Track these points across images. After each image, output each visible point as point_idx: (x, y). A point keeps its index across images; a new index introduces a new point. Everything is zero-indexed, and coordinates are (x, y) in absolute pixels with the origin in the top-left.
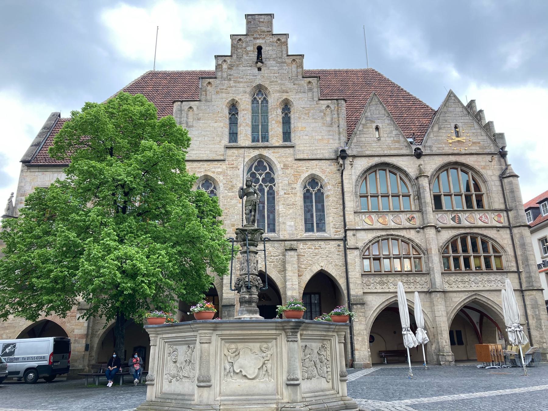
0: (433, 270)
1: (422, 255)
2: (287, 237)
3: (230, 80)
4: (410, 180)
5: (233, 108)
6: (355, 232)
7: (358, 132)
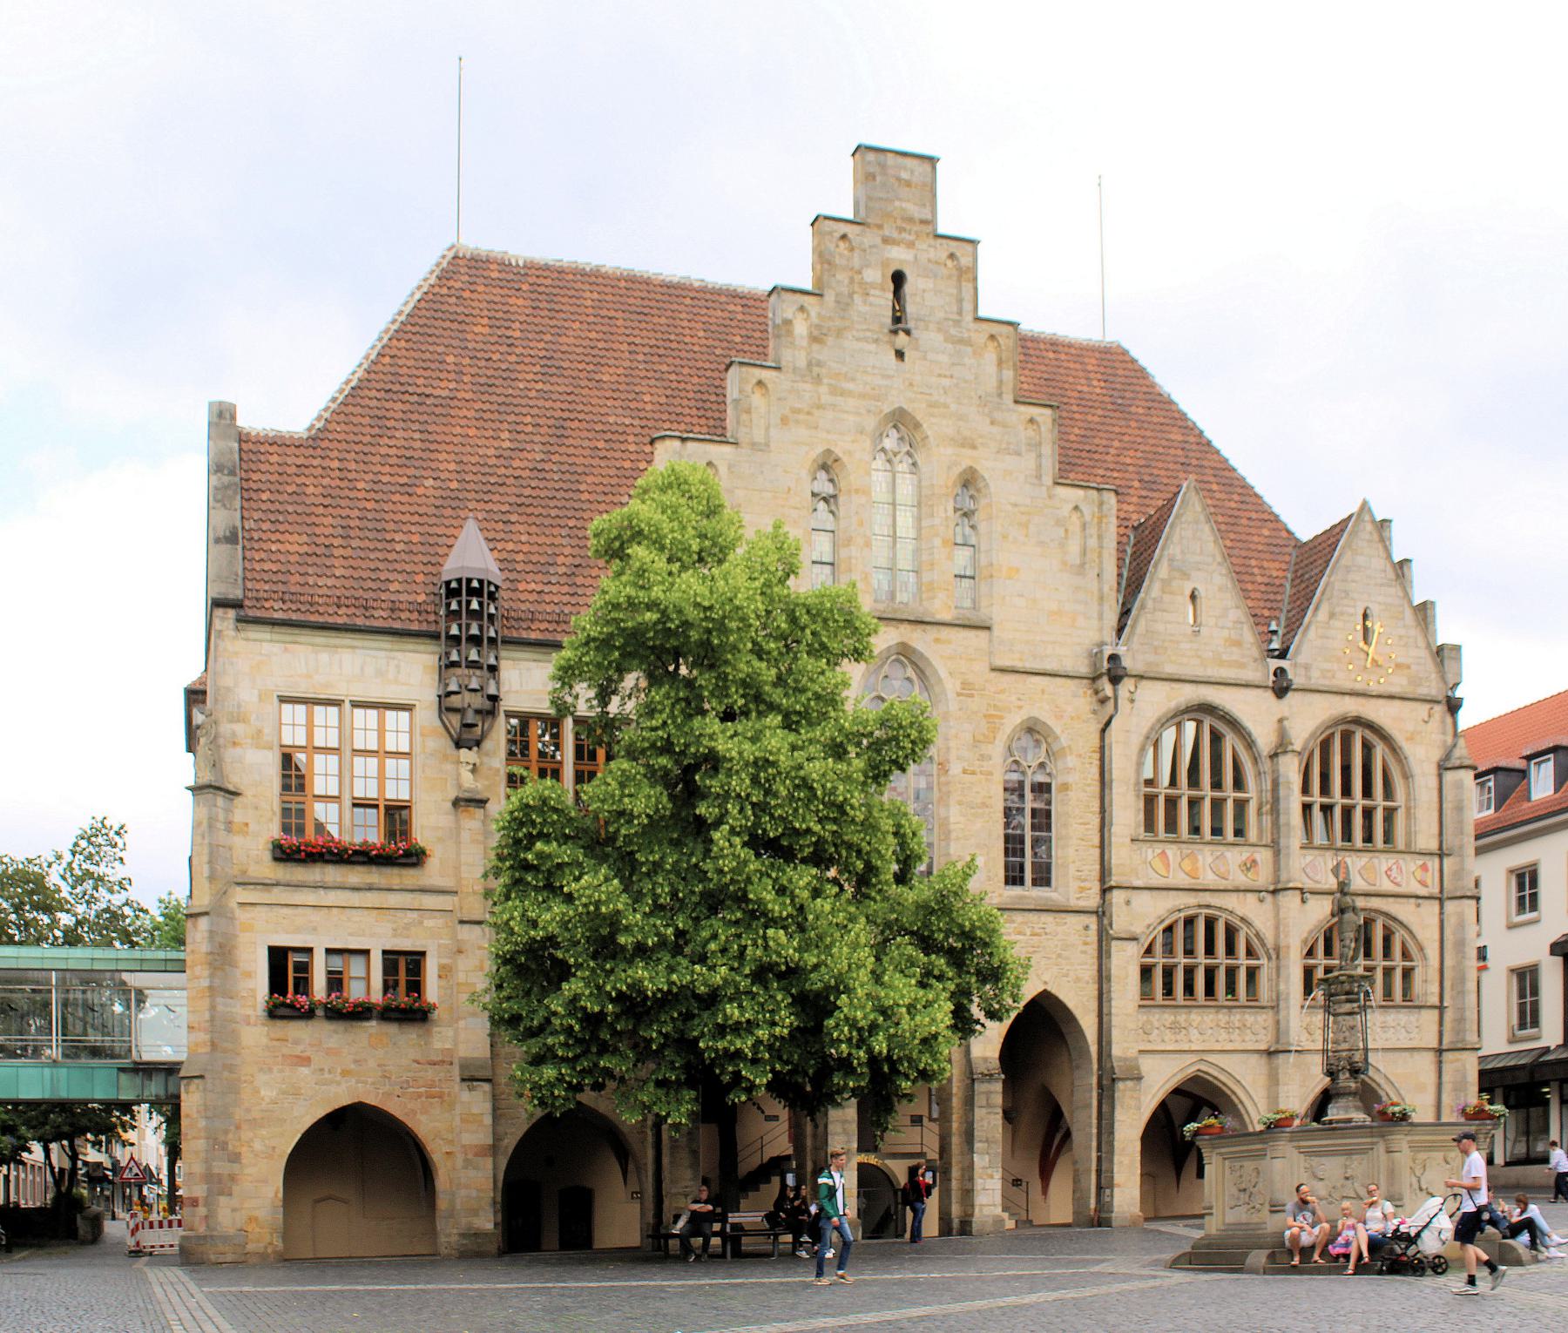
0: (1287, 999)
1: (1263, 961)
3: (818, 380)
4: (1255, 760)
6: (1130, 892)
7: (1150, 604)
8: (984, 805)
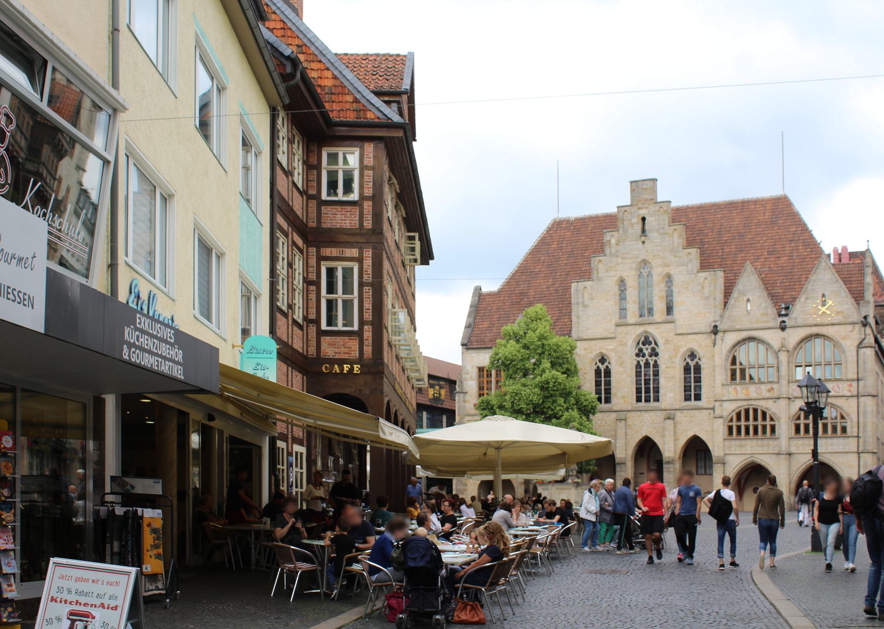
2: (668, 407)
3: (617, 256)
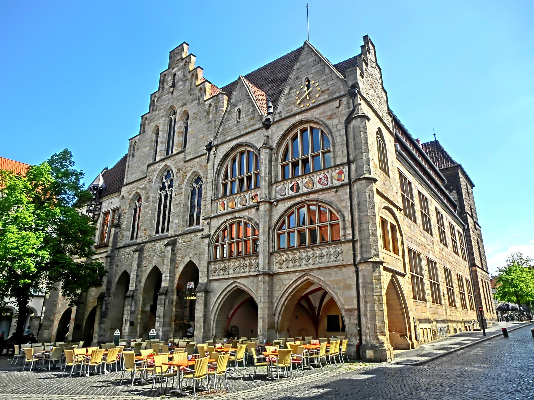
5: (157, 131)
8: (180, 203)
